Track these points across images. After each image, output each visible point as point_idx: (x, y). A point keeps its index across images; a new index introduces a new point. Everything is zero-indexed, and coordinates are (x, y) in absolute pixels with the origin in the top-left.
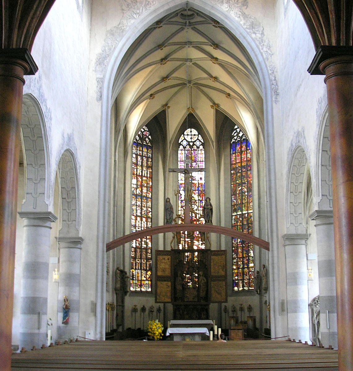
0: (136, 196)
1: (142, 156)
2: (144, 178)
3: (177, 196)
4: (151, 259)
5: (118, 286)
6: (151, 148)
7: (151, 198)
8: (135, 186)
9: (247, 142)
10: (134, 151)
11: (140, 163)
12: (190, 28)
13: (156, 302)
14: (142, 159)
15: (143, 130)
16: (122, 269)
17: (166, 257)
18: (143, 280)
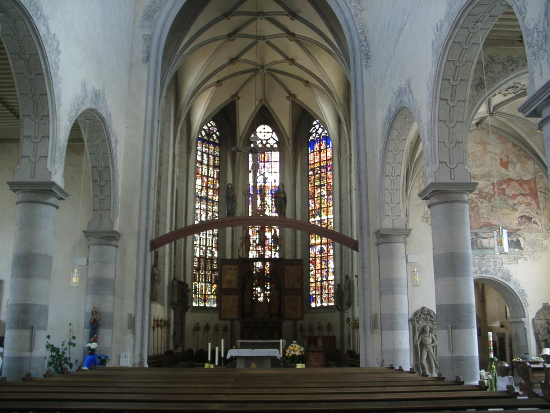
0: (201, 198)
2: (210, 179)
8: (200, 188)
11: (205, 162)
16: (182, 280)
17: (233, 267)
18: (208, 295)
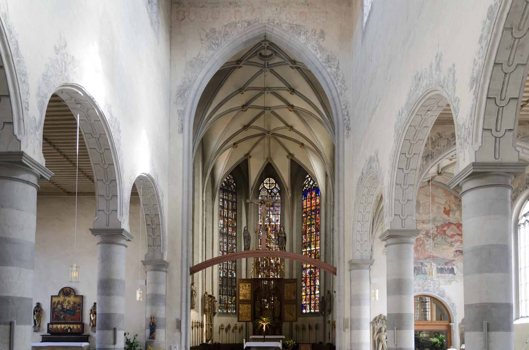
1: (228, 201)
11: (226, 206)
13: (239, 321)
14: (228, 203)
16: (211, 294)
18: (229, 304)
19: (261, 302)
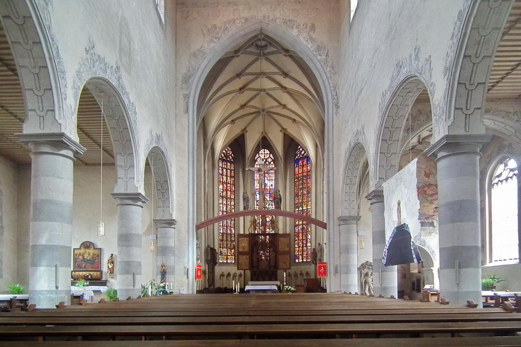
0: (223, 197)
1: (227, 169)
2: (228, 185)
3: (254, 197)
4: (234, 241)
5: (209, 258)
6: (234, 163)
7: (234, 199)
8: (222, 190)
9: (308, 158)
10: (221, 165)
11: (225, 174)
12: (263, 58)
13: (238, 269)
14: (227, 171)
15: (227, 150)
16: (212, 247)
18: (229, 255)
19: (258, 253)
